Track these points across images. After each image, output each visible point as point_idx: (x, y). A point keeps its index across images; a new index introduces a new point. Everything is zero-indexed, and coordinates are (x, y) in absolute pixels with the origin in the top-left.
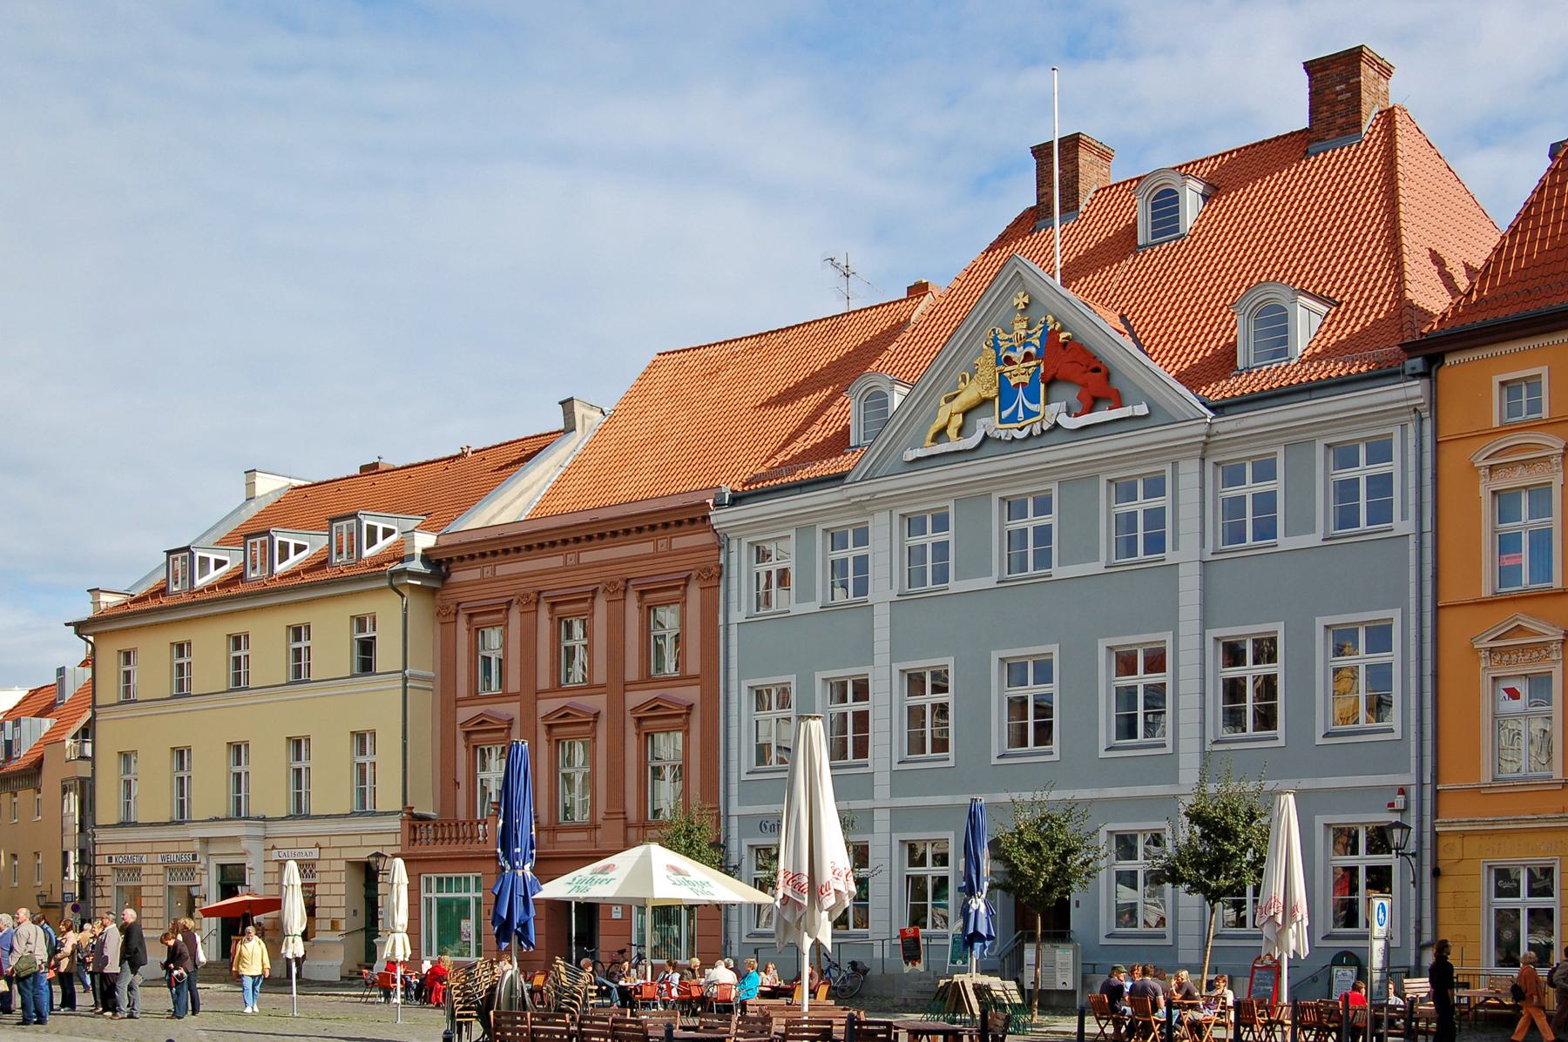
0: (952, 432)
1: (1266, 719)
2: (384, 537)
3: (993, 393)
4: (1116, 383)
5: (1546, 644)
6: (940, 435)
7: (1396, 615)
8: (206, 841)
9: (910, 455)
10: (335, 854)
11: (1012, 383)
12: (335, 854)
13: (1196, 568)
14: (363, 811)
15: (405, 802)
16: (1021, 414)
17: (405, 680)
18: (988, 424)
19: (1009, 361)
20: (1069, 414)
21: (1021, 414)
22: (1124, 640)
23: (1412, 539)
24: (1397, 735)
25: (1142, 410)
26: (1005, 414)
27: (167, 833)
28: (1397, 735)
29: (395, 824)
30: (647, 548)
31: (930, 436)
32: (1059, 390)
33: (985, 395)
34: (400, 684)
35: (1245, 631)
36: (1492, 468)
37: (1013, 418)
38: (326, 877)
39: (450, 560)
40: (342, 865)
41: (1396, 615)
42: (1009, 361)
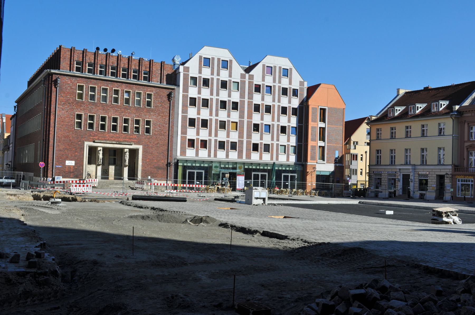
2: (444, 106)
8: (400, 169)
10: (434, 173)
12: (434, 173)
14: (439, 164)
15: (452, 163)
17: (453, 137)
27: (389, 167)
29: (450, 167)
34: (452, 138)
38: (430, 178)
39: (463, 112)
40: (435, 176)
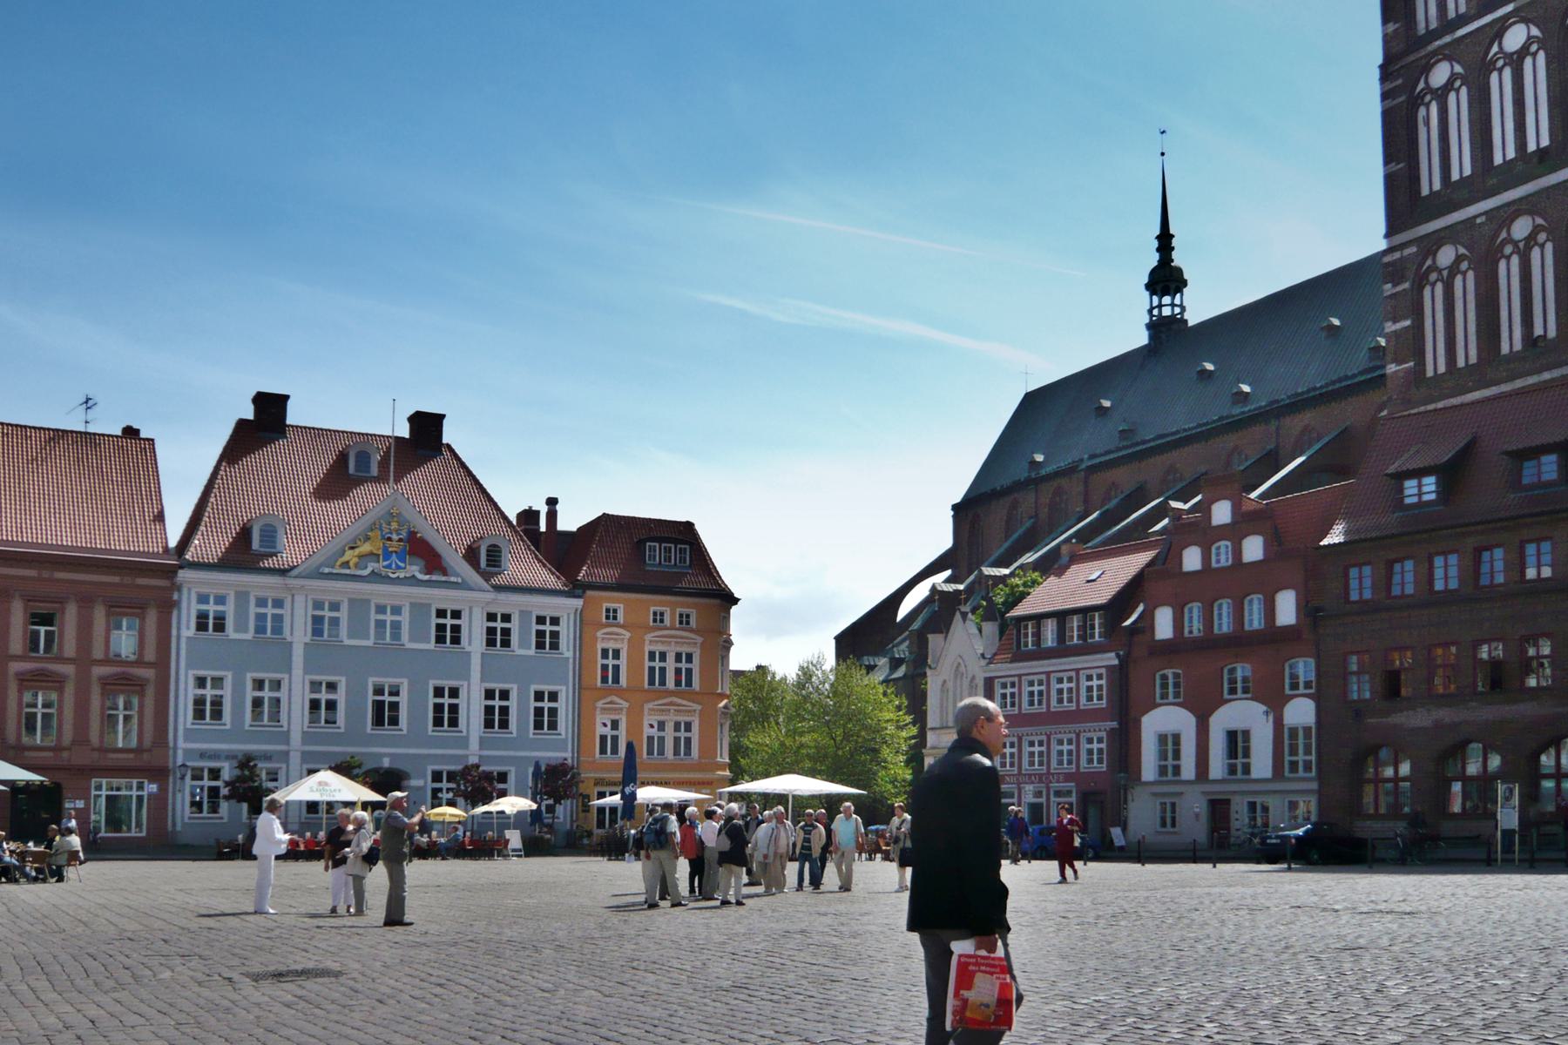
0: (351, 564)
1: (504, 724)
3: (380, 552)
4: (445, 565)
5: (621, 709)
6: (346, 565)
7: (564, 688)
9: (327, 570)
11: (390, 549)
13: (479, 656)
16: (394, 566)
18: (371, 567)
19: (390, 539)
20: (420, 572)
21: (394, 566)
22: (440, 683)
23: (571, 661)
24: (563, 736)
25: (460, 580)
26: (385, 563)
28: (563, 736)
30: (116, 579)
31: (338, 563)
32: (415, 559)
33: (375, 552)
35: (497, 686)
36: (603, 639)
37: (389, 566)
41: (564, 688)
42: (390, 539)
